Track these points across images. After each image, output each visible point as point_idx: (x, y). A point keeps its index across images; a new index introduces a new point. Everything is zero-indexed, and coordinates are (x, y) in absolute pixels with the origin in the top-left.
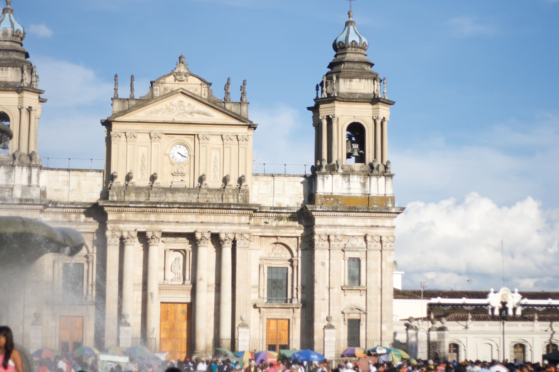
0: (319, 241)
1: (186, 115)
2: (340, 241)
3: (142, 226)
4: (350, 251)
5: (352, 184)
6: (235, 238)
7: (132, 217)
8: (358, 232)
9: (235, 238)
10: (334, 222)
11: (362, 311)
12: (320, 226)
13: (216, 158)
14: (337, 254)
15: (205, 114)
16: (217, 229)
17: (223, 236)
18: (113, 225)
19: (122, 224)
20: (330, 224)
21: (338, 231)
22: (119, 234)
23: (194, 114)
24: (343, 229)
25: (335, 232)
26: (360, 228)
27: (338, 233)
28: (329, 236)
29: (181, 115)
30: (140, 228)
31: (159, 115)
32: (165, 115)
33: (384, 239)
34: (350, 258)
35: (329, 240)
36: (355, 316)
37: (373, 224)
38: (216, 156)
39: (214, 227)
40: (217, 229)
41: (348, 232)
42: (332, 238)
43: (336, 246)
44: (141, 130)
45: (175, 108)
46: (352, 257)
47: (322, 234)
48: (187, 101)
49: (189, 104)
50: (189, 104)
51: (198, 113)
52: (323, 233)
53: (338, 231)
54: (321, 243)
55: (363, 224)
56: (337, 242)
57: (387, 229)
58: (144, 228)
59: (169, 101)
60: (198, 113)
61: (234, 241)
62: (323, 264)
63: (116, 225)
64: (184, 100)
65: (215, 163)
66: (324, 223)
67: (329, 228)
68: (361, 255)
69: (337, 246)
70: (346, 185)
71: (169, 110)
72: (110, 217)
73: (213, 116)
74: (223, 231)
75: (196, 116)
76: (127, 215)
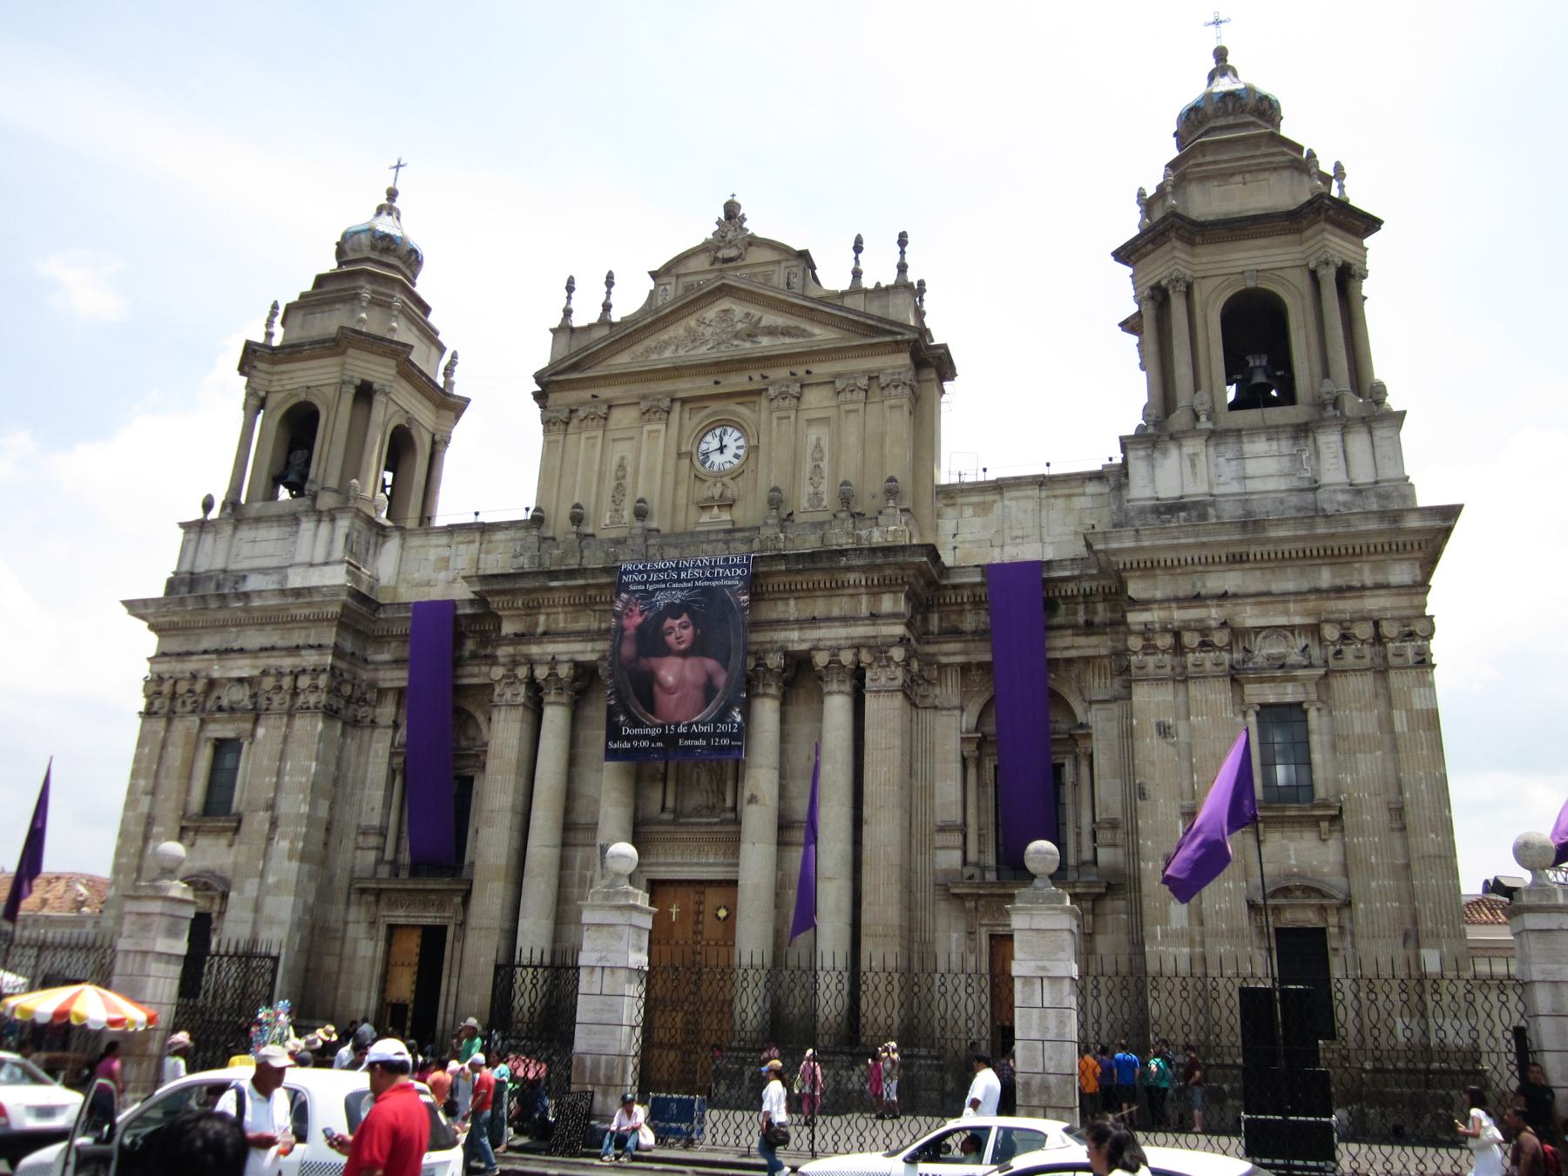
0: (1146, 654)
1: (736, 342)
2: (1221, 649)
3: (589, 646)
4: (1261, 680)
5: (1252, 467)
6: (858, 663)
7: (566, 621)
8: (1287, 613)
9: (858, 663)
10: (1194, 585)
11: (1331, 897)
12: (1145, 604)
13: (818, 446)
14: (1216, 695)
15: (786, 332)
16: (803, 641)
17: (821, 659)
18: (511, 650)
19: (534, 643)
20: (1181, 594)
21: (1213, 614)
22: (522, 672)
23: (760, 339)
24: (1228, 605)
25: (1201, 620)
26: (1292, 598)
27: (1213, 624)
28: (1177, 635)
29: (723, 348)
30: (582, 652)
31: (668, 354)
32: (681, 352)
33: (1388, 629)
34: (1263, 706)
35: (1179, 649)
36: (1306, 917)
37: (1339, 582)
38: (818, 439)
39: (795, 635)
40: (803, 641)
41: (1250, 617)
42: (1191, 639)
43: (1208, 665)
44: (618, 398)
45: (709, 331)
46: (1272, 699)
47: (1153, 631)
48: (738, 309)
49: (747, 314)
50: (747, 314)
51: (771, 331)
52: (1157, 626)
53: (1213, 614)
54: (1151, 661)
55: (1305, 586)
56: (1212, 654)
57: (1398, 595)
58: (593, 651)
59: (696, 316)
60: (771, 331)
61: (858, 675)
62: (1164, 730)
63: (519, 647)
64: (734, 307)
65: (814, 459)
66: (1159, 595)
67: (1179, 608)
68: (1307, 693)
69: (1215, 668)
70: (1229, 470)
71: (694, 338)
72: (508, 628)
73: (813, 335)
74: (821, 644)
75: (765, 341)
76: (552, 617)
